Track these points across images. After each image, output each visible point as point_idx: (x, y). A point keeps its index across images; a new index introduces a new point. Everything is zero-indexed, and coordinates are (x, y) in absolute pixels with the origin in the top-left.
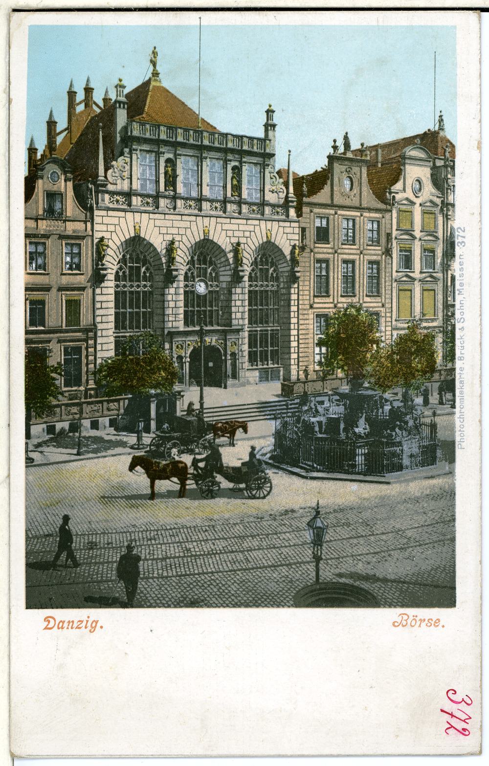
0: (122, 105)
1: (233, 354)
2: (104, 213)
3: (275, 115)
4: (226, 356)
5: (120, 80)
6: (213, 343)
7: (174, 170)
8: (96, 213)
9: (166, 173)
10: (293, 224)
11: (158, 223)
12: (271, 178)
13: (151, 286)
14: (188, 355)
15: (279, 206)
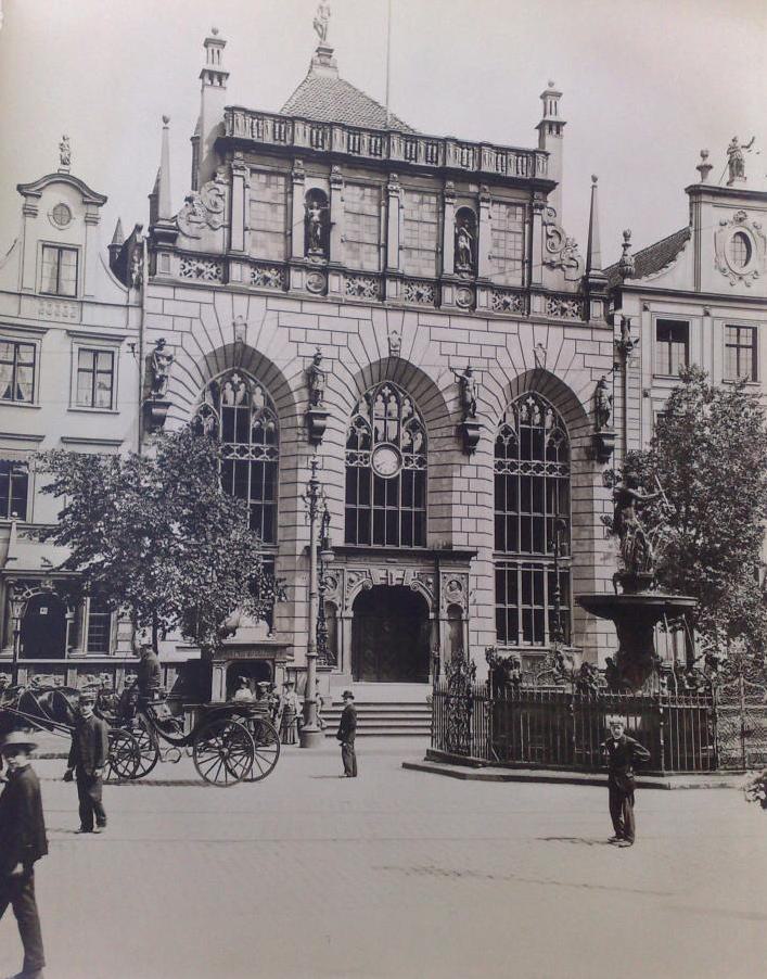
0: (215, 80)
1: (455, 609)
2: (168, 292)
3: (561, 103)
4: (437, 610)
5: (215, 32)
6: (409, 582)
7: (326, 215)
8: (149, 291)
9: (307, 220)
10: (599, 335)
11: (285, 320)
12: (549, 236)
13: (272, 453)
14: (350, 604)
15: (565, 296)
